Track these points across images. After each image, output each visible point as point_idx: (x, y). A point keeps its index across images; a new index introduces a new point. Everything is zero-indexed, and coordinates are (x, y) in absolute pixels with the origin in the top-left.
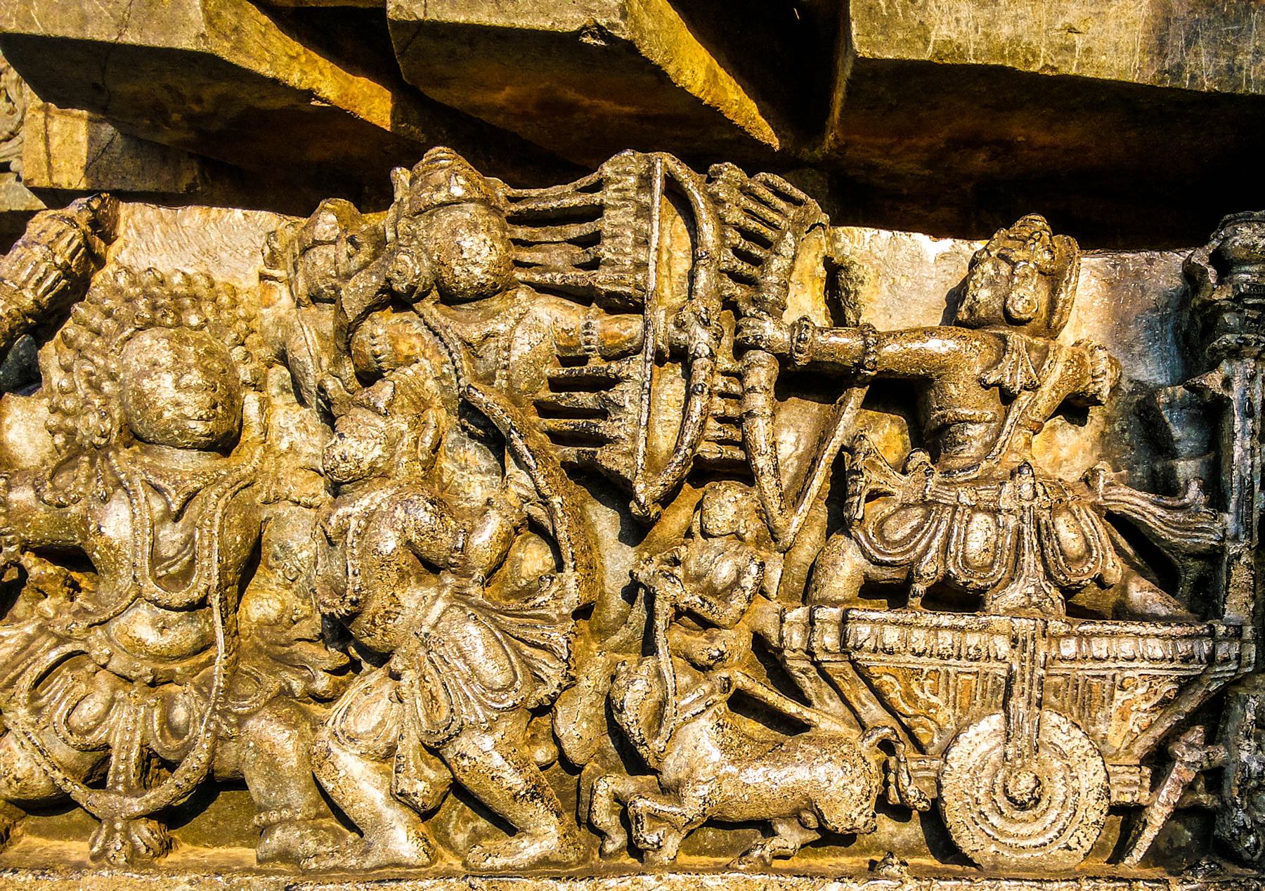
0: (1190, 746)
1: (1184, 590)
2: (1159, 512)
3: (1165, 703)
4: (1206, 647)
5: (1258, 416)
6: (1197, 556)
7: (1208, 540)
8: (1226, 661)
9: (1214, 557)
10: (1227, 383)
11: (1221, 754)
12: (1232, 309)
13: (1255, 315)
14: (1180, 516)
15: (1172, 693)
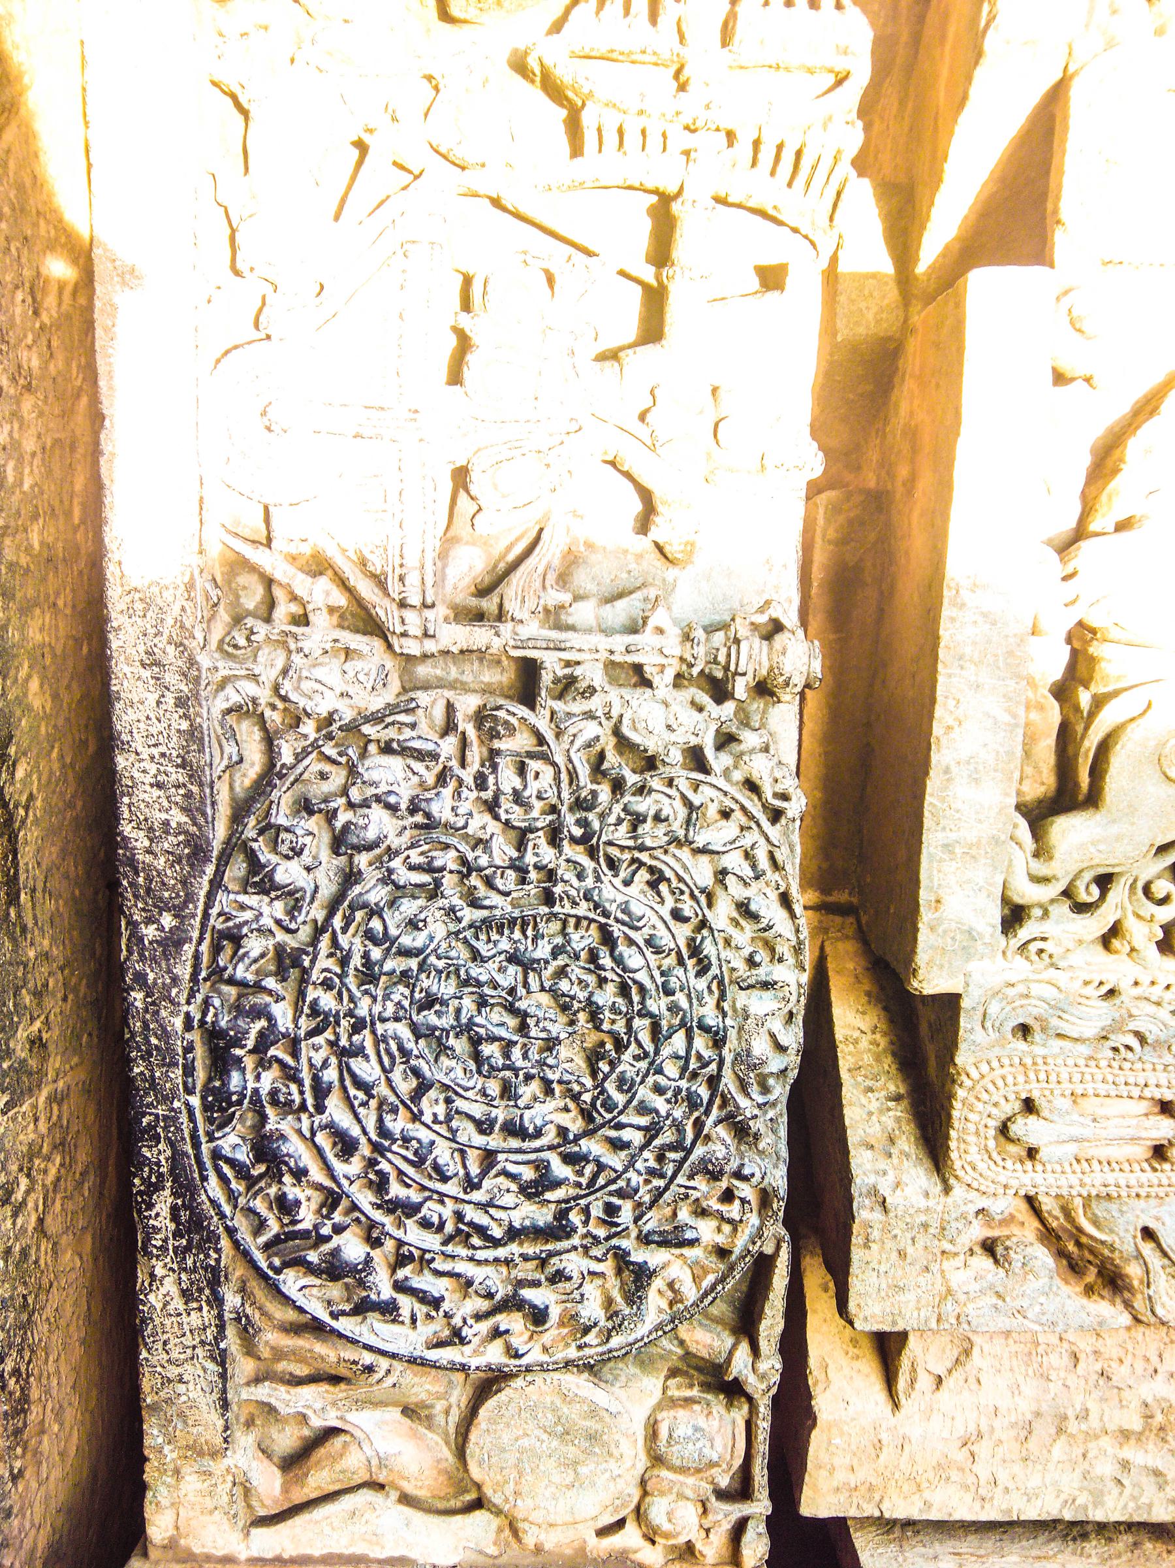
0: (328, 594)
1: (474, 602)
2: (541, 570)
3: (363, 563)
4: (414, 599)
5: (630, 659)
6: (501, 606)
7: (511, 606)
8: (403, 622)
9: (501, 616)
10: (660, 631)
11: (322, 622)
12: (728, 639)
13: (722, 658)
14: (538, 584)
15: (372, 569)
